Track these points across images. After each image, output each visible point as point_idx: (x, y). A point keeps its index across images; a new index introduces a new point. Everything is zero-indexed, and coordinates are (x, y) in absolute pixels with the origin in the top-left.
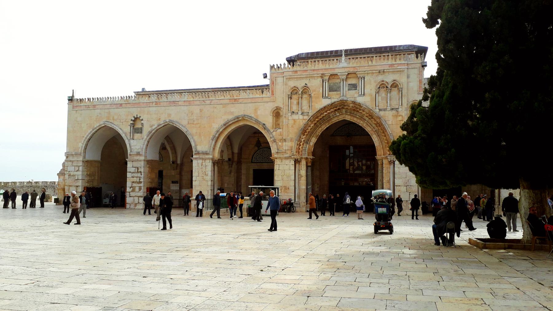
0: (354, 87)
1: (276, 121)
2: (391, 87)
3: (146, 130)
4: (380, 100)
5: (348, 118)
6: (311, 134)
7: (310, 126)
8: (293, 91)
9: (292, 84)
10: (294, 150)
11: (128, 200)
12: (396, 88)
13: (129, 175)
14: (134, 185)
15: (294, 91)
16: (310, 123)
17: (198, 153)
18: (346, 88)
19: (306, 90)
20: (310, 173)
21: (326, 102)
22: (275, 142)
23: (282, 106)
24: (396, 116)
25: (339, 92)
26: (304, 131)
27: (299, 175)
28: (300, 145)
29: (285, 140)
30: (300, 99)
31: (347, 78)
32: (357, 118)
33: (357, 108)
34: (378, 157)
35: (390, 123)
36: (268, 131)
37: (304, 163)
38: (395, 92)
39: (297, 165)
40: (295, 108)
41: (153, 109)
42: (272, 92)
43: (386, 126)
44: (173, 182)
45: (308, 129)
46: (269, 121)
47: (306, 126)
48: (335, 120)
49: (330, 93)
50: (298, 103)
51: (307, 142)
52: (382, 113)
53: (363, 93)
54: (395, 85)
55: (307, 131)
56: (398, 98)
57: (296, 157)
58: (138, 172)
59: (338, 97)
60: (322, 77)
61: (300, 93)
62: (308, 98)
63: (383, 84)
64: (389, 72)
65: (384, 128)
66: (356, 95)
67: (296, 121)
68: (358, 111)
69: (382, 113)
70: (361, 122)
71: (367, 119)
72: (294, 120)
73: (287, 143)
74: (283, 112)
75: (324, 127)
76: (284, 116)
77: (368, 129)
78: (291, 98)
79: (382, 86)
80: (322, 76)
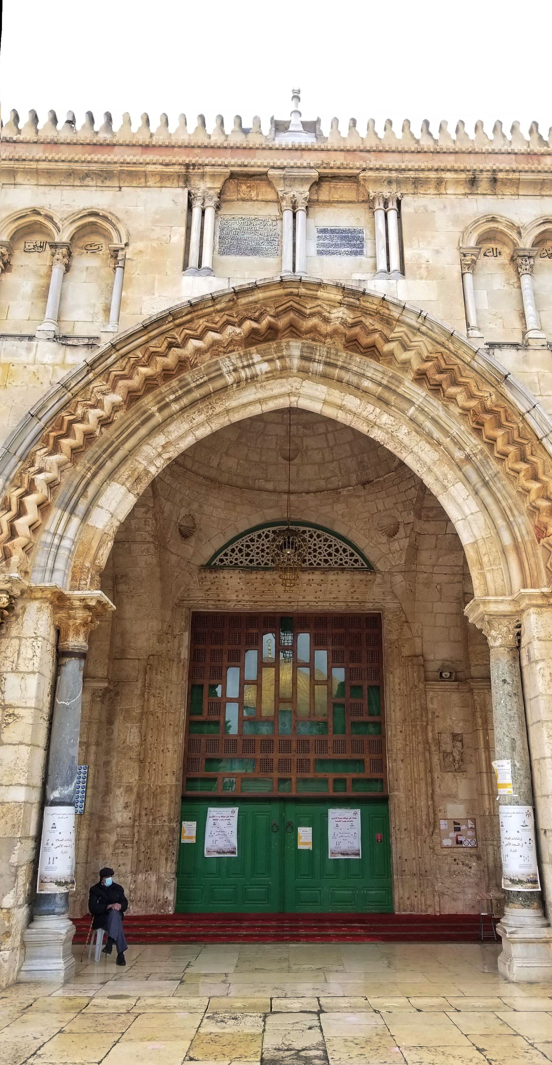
4: (485, 305)
5: (314, 397)
6: (97, 455)
16: (99, 385)
18: (307, 246)
19: (92, 227)
30: (58, 270)
48: (247, 403)
50: (44, 293)
51: (76, 499)
52: (506, 360)
53: (395, 264)
68: (372, 351)
70: (385, 419)
71: (419, 394)
75: (185, 433)
77: (420, 458)
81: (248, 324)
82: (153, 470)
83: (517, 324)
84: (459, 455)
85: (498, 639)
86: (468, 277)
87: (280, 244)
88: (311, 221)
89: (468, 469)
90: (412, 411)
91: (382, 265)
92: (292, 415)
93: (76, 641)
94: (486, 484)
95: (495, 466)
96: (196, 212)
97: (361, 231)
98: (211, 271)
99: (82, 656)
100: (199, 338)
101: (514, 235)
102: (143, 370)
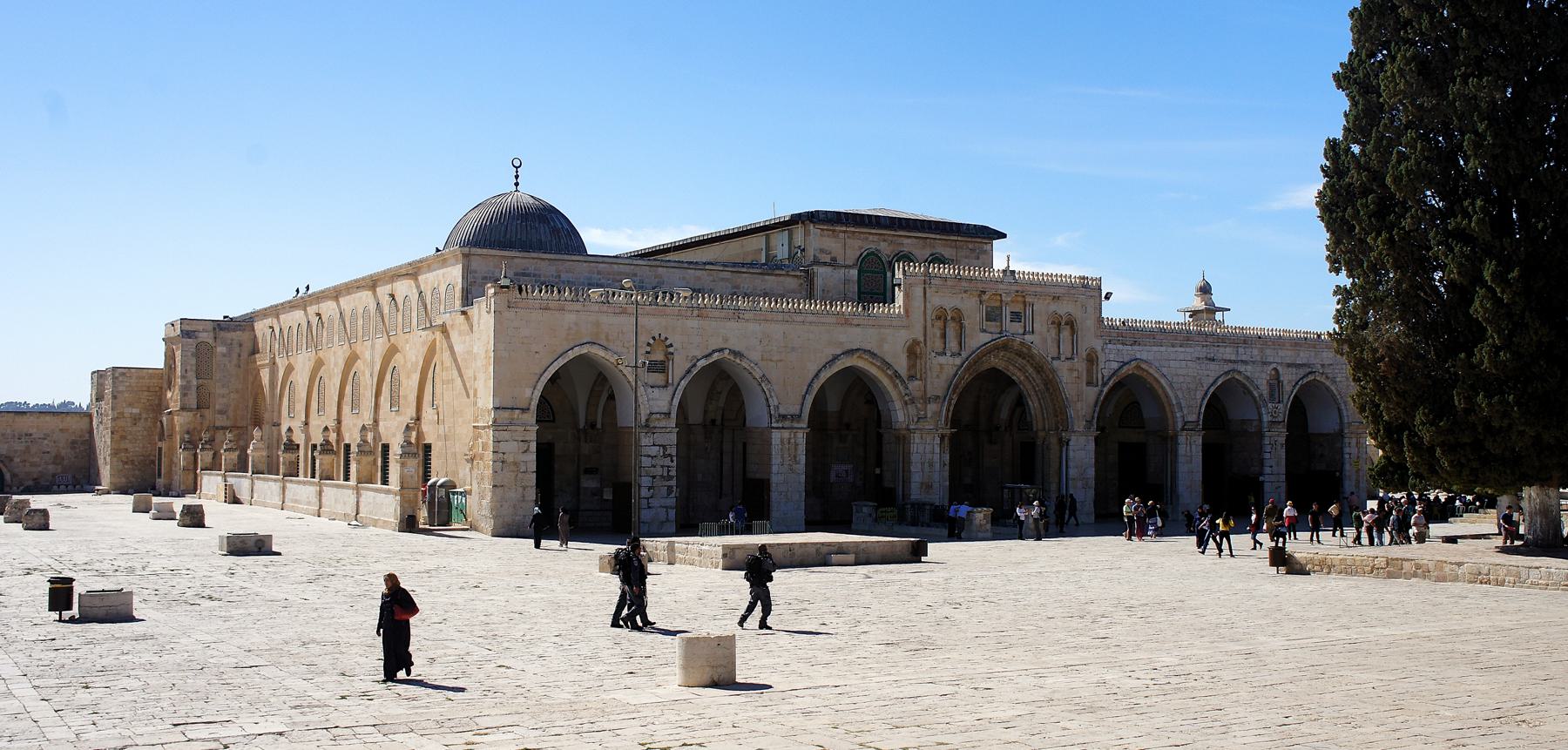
0: (1016, 317)
3: (679, 367)
9: (936, 300)
11: (646, 515)
13: (646, 462)
14: (658, 482)
17: (784, 417)
33: (1025, 353)
36: (903, 381)
37: (946, 440)
38: (1066, 334)
40: (938, 344)
41: (694, 323)
44: (587, 471)
46: (901, 365)
50: (944, 336)
54: (1071, 323)
58: (665, 456)
67: (943, 368)
69: (1056, 363)
72: (941, 365)
79: (1056, 323)
92: (994, 369)
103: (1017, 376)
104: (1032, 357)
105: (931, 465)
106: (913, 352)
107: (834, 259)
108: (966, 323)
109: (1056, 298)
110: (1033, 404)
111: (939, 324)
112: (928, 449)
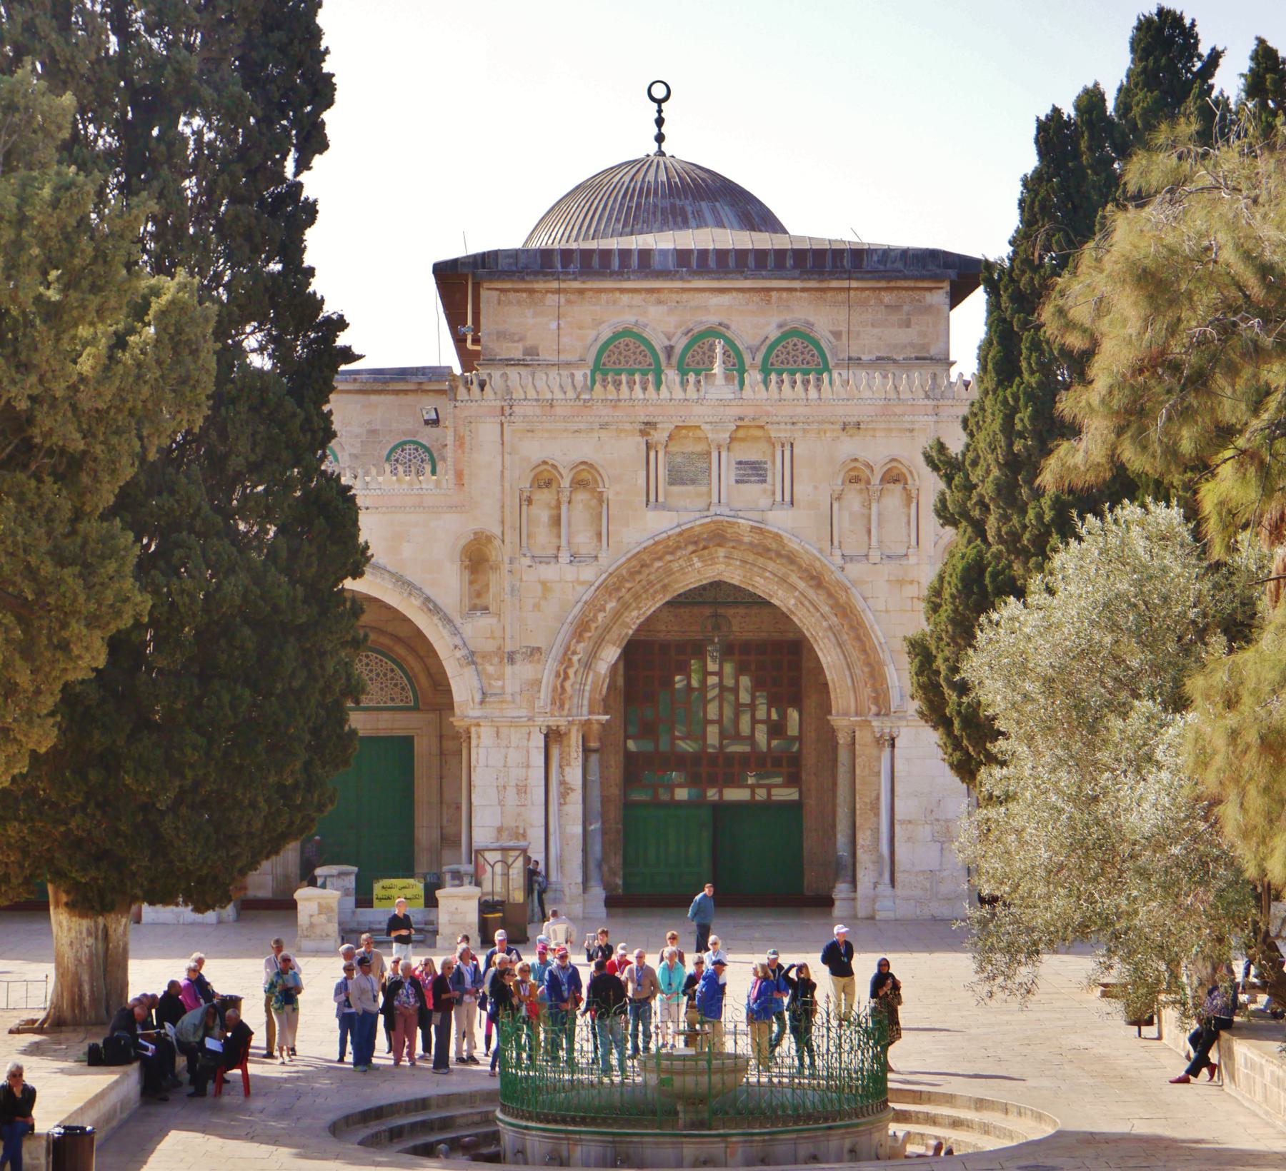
0: (753, 471)
1: (471, 583)
2: (882, 480)
5: (734, 576)
7: (603, 609)
8: (535, 476)
9: (535, 450)
10: (545, 694)
12: (899, 486)
15: (544, 478)
18: (729, 475)
20: (594, 777)
21: (659, 524)
22: (474, 663)
23: (497, 530)
24: (901, 582)
25: (704, 489)
26: (581, 629)
27: (562, 783)
28: (566, 677)
29: (511, 660)
31: (732, 439)
32: (765, 578)
33: (768, 547)
34: (837, 720)
35: (881, 605)
36: (447, 620)
37: (575, 739)
38: (893, 499)
39: (555, 752)
40: (543, 537)
42: (459, 475)
43: (868, 618)
45: (595, 619)
47: (593, 606)
49: (676, 489)
50: (556, 521)
53: (787, 498)
55: (593, 626)
56: (904, 519)
57: (552, 722)
59: (701, 504)
60: (643, 433)
61: (566, 483)
62: (594, 502)
63: (854, 469)
64: (874, 429)
65: (861, 624)
66: (764, 502)
69: (854, 570)
70: (780, 592)
71: (801, 585)
72: (544, 584)
73: (517, 667)
74: (501, 553)
76: (507, 567)
78: (530, 501)
80: (647, 428)
81: (691, 548)
82: (631, 632)
83: (866, 538)
84: (825, 624)
85: (842, 739)
86: (836, 506)
87: (710, 476)
88: (731, 454)
89: (830, 634)
90: (797, 593)
91: (778, 498)
92: (717, 585)
93: (594, 744)
94: (840, 645)
95: (845, 637)
96: (652, 454)
97: (765, 463)
98: (664, 507)
99: (595, 751)
100: (660, 559)
101: (868, 472)
102: (628, 585)
103: (782, 599)
104: (791, 559)
105: (522, 789)
106: (476, 559)
107: (532, 351)
108: (611, 492)
109: (851, 427)
110: (828, 656)
111: (545, 496)
112: (514, 757)
